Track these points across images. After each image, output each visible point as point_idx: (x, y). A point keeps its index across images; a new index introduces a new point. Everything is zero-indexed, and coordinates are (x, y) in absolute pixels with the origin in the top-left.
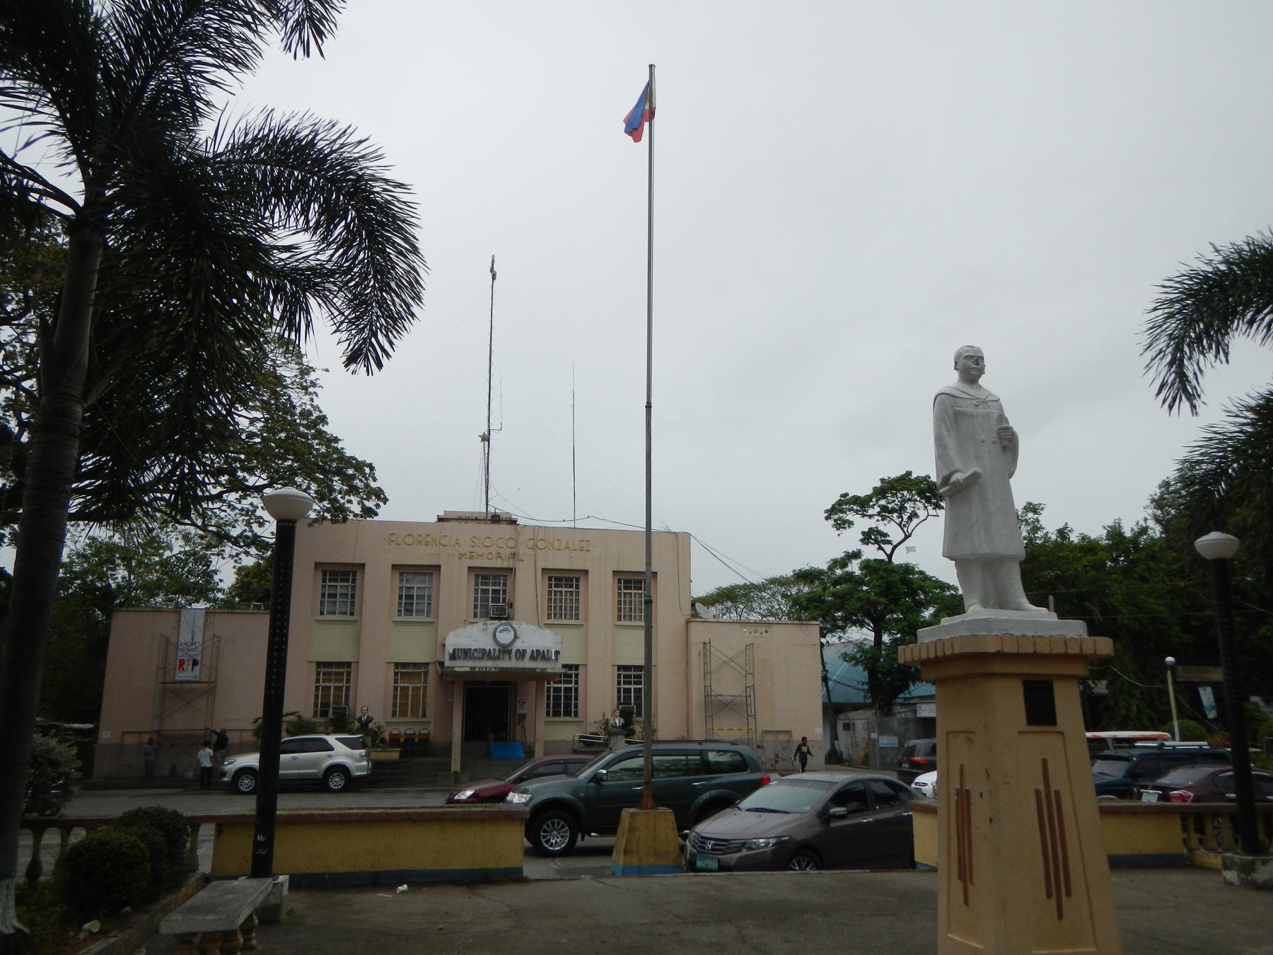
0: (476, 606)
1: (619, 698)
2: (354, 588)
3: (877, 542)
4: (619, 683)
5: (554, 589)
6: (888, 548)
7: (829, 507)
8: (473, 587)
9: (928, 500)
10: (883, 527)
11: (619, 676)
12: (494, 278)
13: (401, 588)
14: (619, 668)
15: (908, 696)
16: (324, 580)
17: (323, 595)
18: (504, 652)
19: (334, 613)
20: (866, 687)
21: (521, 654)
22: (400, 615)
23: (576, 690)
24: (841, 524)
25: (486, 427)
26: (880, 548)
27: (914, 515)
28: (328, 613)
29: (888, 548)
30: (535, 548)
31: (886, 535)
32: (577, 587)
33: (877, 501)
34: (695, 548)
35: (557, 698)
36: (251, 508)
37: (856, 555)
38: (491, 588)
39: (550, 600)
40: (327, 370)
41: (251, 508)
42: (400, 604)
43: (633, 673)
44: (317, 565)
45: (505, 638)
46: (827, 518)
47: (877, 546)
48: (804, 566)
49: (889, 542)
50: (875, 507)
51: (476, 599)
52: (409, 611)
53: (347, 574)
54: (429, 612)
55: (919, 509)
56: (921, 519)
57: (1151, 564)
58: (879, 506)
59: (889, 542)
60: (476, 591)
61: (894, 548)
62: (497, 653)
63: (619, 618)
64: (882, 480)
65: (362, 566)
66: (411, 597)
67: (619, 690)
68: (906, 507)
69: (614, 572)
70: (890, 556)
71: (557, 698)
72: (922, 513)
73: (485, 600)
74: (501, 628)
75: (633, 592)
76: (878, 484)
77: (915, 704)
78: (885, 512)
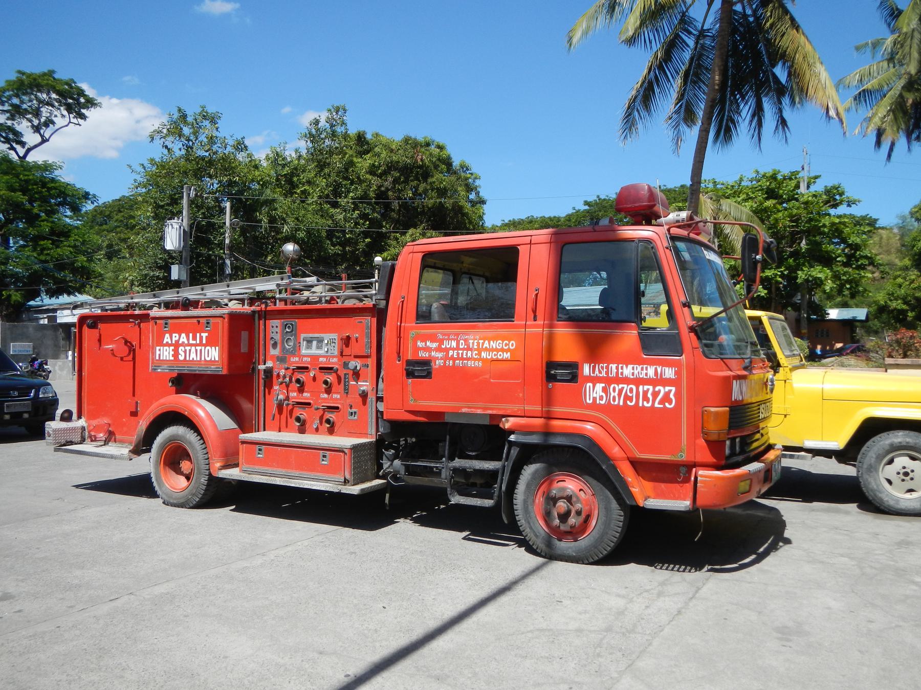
6: (21, 151)
9: (69, 109)
15: (40, 303)
27: (49, 122)
29: (21, 151)
31: (17, 134)
33: (10, 98)
47: (7, 146)
50: (6, 104)
55: (56, 116)
56: (57, 126)
57: (307, 187)
58: (12, 105)
59: (23, 144)
61: (29, 150)
68: (42, 111)
72: (59, 121)
76: (13, 77)
77: (55, 310)
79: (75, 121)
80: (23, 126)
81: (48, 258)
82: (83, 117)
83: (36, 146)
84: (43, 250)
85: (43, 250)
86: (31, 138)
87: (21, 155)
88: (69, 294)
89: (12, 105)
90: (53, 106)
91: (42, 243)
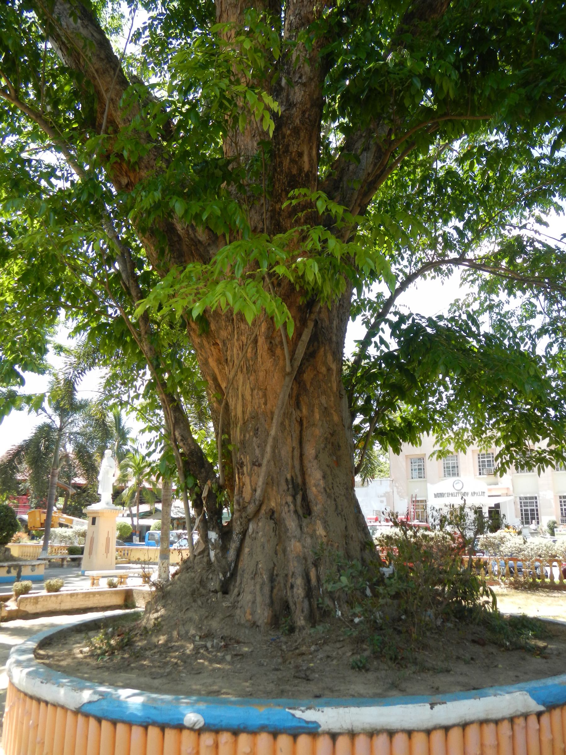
1: (562, 514)
4: (561, 505)
11: (561, 502)
14: (560, 497)
23: (537, 510)
35: (527, 515)
38: (486, 459)
45: (458, 487)
51: (479, 466)
60: (479, 462)
67: (562, 510)
71: (527, 515)
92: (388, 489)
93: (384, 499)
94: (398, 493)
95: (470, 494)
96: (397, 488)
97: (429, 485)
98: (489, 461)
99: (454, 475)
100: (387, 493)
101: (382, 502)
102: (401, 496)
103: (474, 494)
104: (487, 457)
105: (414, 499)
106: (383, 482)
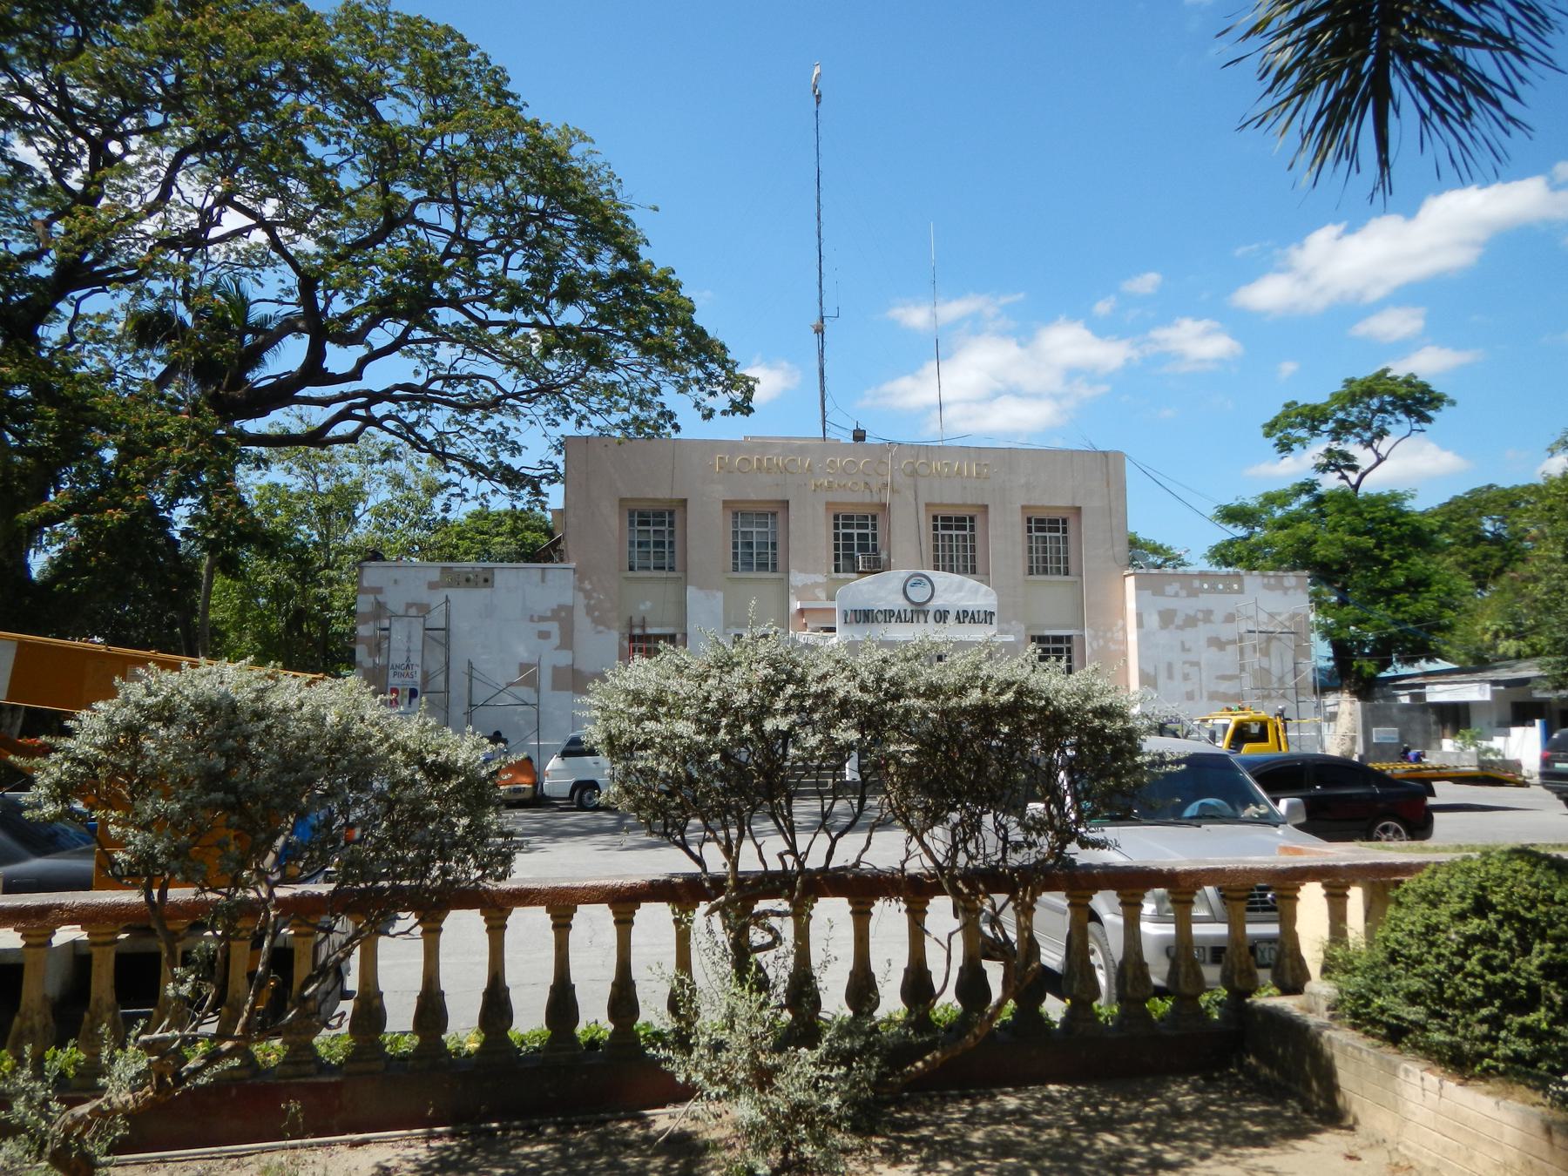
0: (837, 557)
2: (672, 533)
3: (1338, 468)
5: (941, 532)
6: (1353, 477)
7: (1269, 419)
8: (832, 531)
9: (1408, 411)
10: (1334, 445)
12: (818, 97)
13: (735, 533)
16: (631, 523)
17: (632, 543)
18: (918, 612)
19: (648, 568)
20: (1332, 663)
21: (942, 616)
22: (735, 569)
24: (1285, 447)
25: (818, 314)
26: (1344, 477)
28: (641, 568)
30: (914, 474)
32: (972, 528)
34: (1132, 475)
36: (500, 430)
37: (1308, 487)
38: (855, 531)
39: (936, 548)
40: (656, 209)
41: (500, 430)
42: (735, 555)
43: (1051, 646)
44: (622, 500)
45: (918, 594)
46: (1267, 435)
47: (1338, 474)
48: (1231, 500)
49: (1354, 468)
51: (837, 547)
52: (748, 566)
53: (661, 514)
54: (774, 565)
58: (1337, 421)
59: (1354, 468)
60: (836, 537)
61: (1363, 475)
62: (909, 615)
63: (1031, 573)
64: (1350, 382)
65: (685, 501)
66: (750, 545)
69: (1023, 507)
70: (1356, 487)
73: (848, 547)
74: (912, 581)
75: (1048, 534)
76: (1338, 387)
77: (1423, 686)
78: (1343, 429)
79: (1416, 426)
80: (1353, 447)
81: (1406, 616)
82: (1429, 420)
83: (1371, 469)
84: (1399, 605)
85: (1399, 605)
86: (1364, 457)
87: (1354, 482)
88: (1429, 659)
89: (1337, 421)
90: (1386, 411)
91: (1397, 597)
92: (567, 597)
93: (553, 627)
94: (590, 610)
95: (951, 618)
96: (588, 595)
97: (692, 592)
98: (862, 537)
99: (763, 566)
100: (561, 607)
101: (544, 635)
102: (597, 621)
103: (964, 616)
104: (860, 526)
105: (637, 631)
106: (550, 575)
